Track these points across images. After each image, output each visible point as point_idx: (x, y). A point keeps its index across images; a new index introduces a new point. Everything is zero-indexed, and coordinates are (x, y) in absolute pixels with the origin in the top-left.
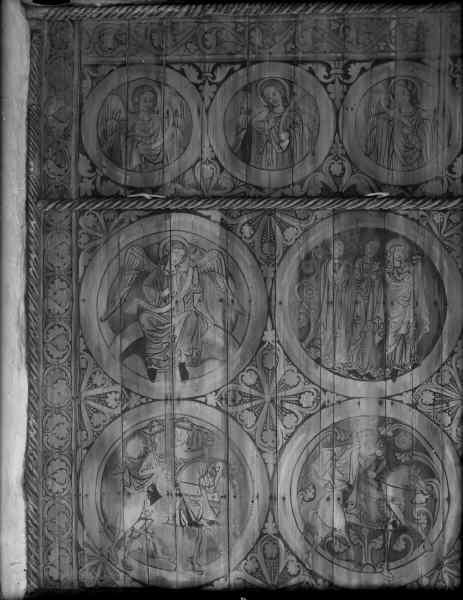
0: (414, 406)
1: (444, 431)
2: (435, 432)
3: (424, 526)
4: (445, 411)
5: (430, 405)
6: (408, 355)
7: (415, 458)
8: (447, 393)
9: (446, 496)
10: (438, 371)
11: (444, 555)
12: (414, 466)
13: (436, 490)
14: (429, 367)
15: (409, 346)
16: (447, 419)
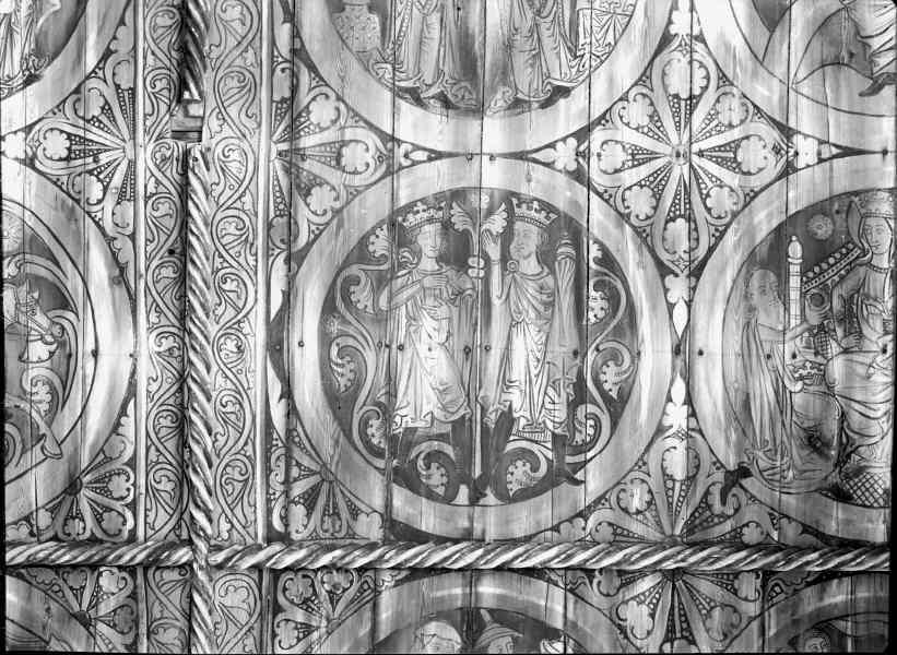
0: (30, 162)
1: (89, 213)
2: (71, 215)
3: (44, 407)
4: (90, 172)
5: (61, 160)
6: (17, 58)
7: (29, 269)
8: (95, 135)
9: (90, 346)
10: (77, 91)
11: (84, 465)
12: (25, 288)
13: (71, 332)
14: (59, 81)
15: (17, 37)
16: (96, 191)
